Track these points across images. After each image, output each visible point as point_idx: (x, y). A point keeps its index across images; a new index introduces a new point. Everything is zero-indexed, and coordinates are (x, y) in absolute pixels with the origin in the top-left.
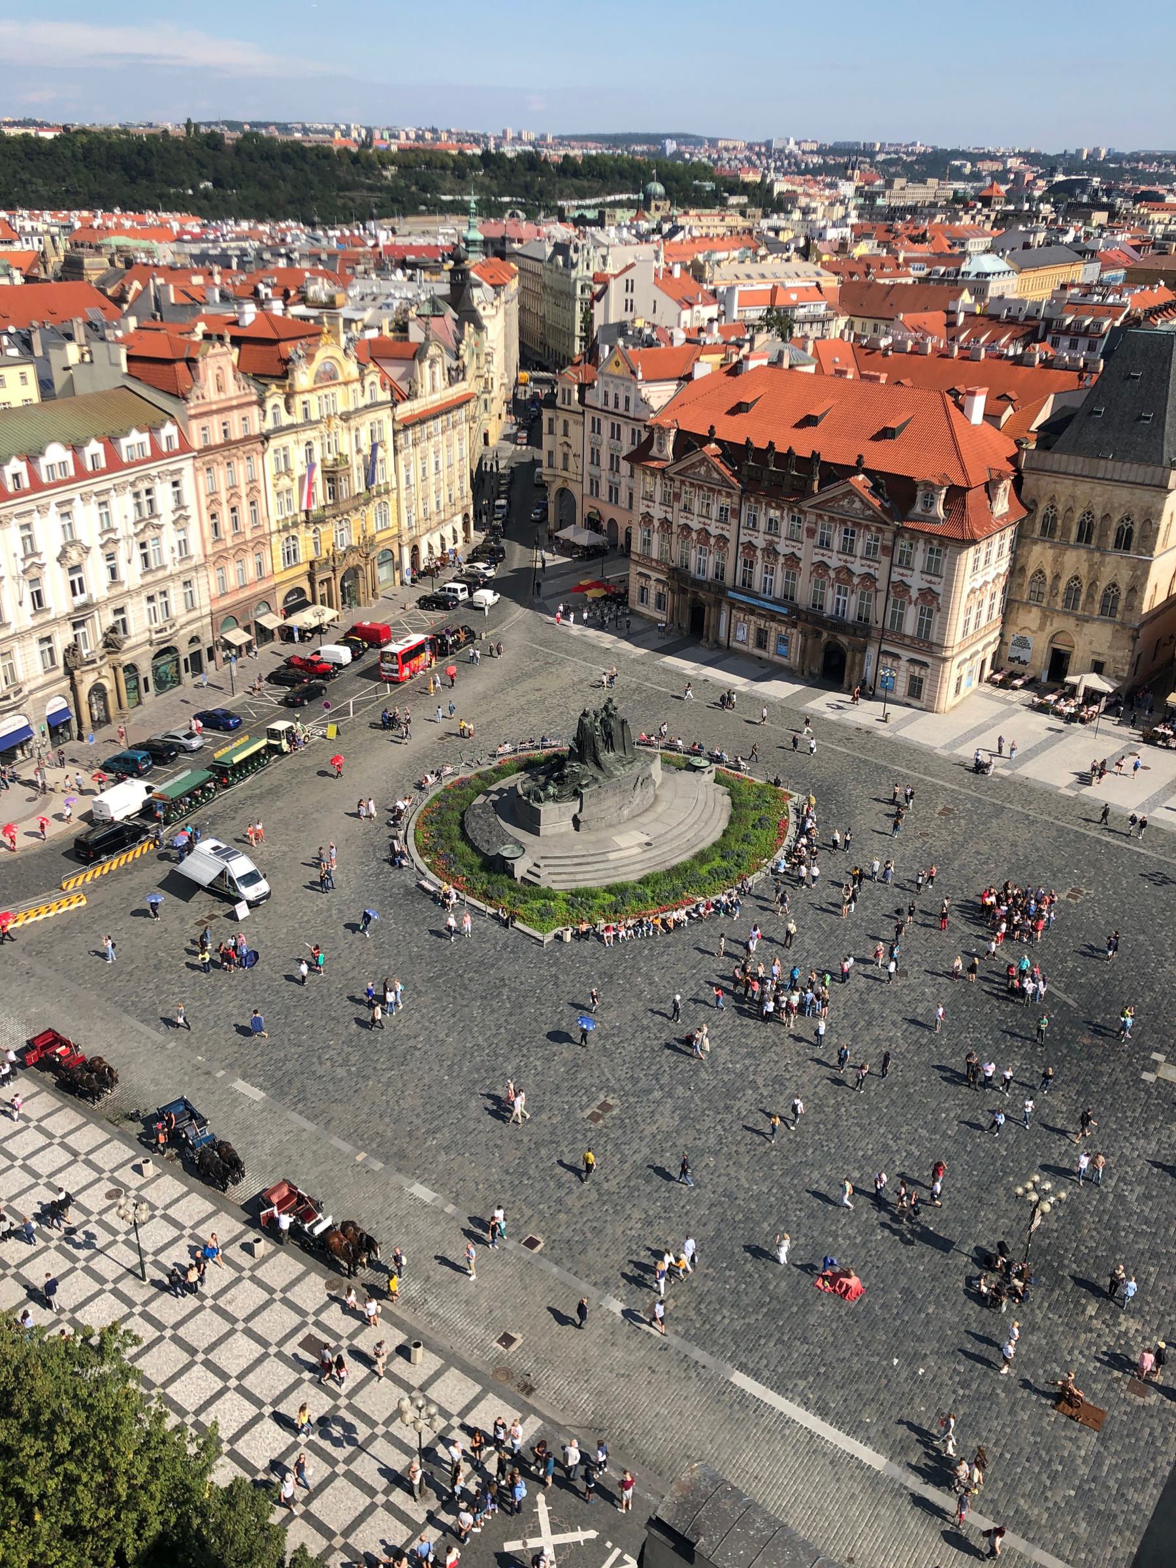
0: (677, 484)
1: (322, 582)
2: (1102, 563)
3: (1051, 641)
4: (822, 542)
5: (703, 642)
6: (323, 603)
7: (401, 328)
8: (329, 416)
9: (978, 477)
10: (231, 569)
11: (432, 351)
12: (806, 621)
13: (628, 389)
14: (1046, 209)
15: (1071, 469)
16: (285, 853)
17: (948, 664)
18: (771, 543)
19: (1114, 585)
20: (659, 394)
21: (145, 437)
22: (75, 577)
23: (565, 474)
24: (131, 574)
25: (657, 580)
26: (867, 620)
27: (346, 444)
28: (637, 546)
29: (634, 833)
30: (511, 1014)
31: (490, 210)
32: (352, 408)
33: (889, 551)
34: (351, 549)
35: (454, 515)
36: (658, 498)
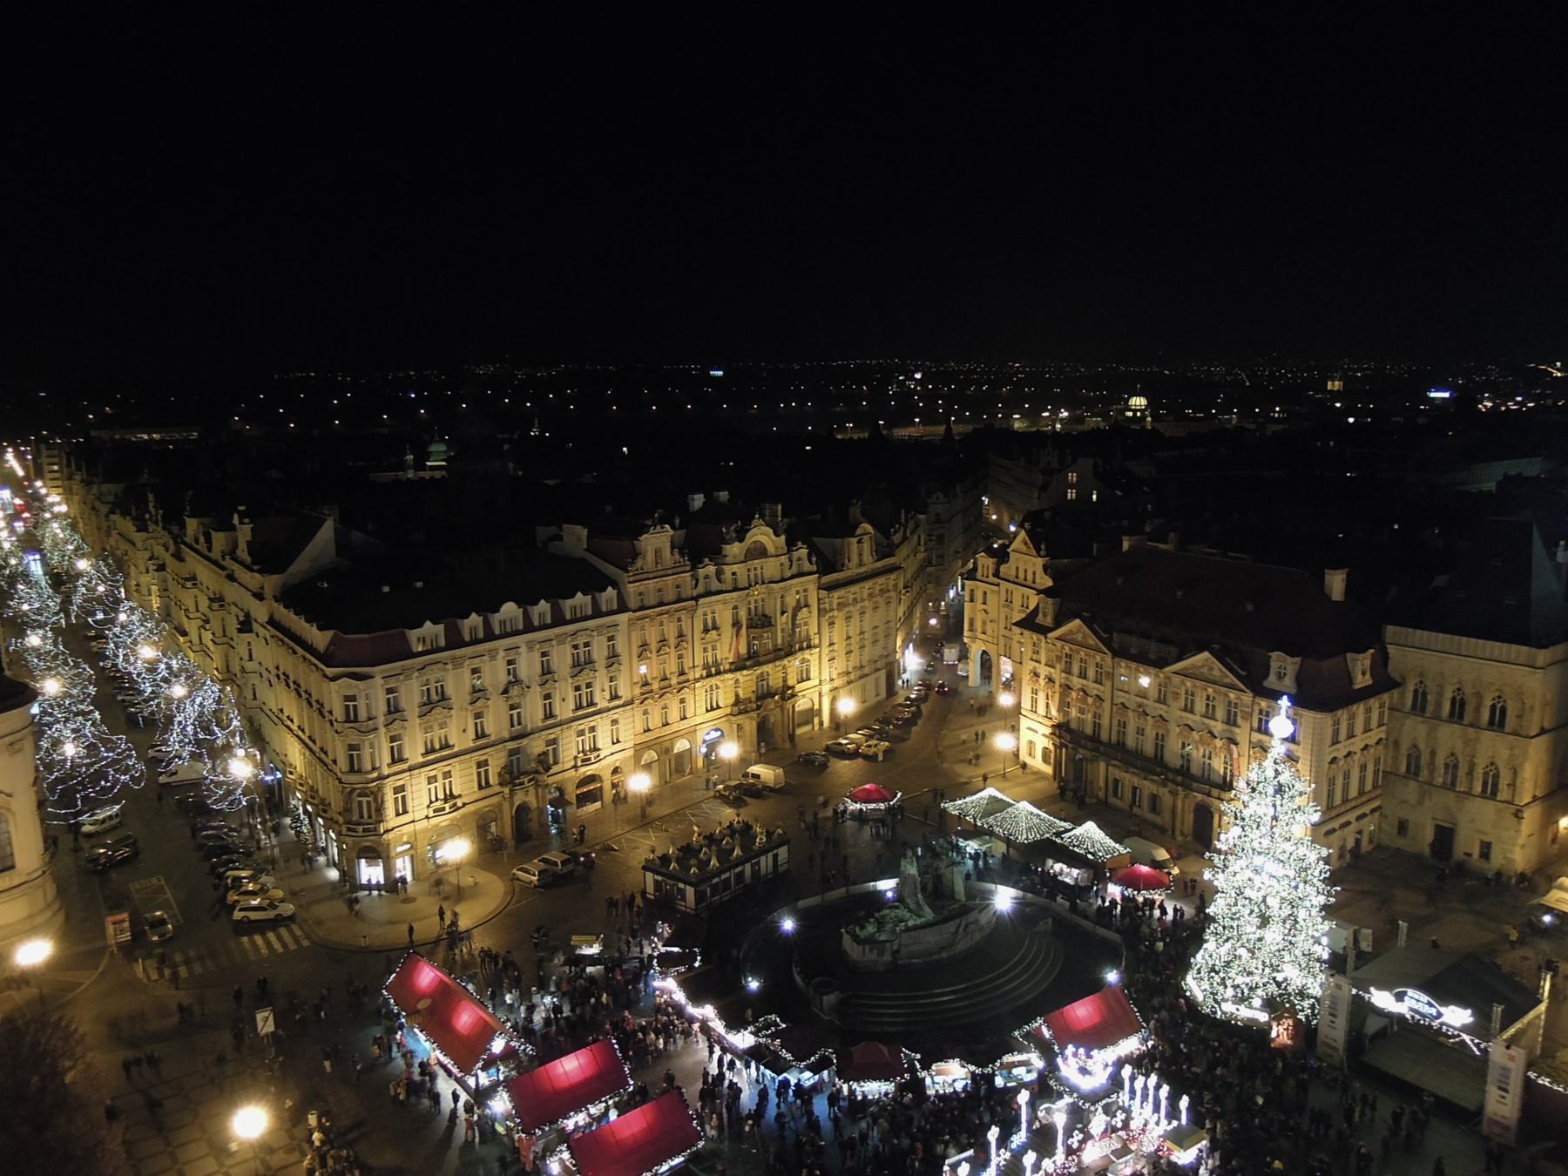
22: (514, 712)
35: (877, 670)
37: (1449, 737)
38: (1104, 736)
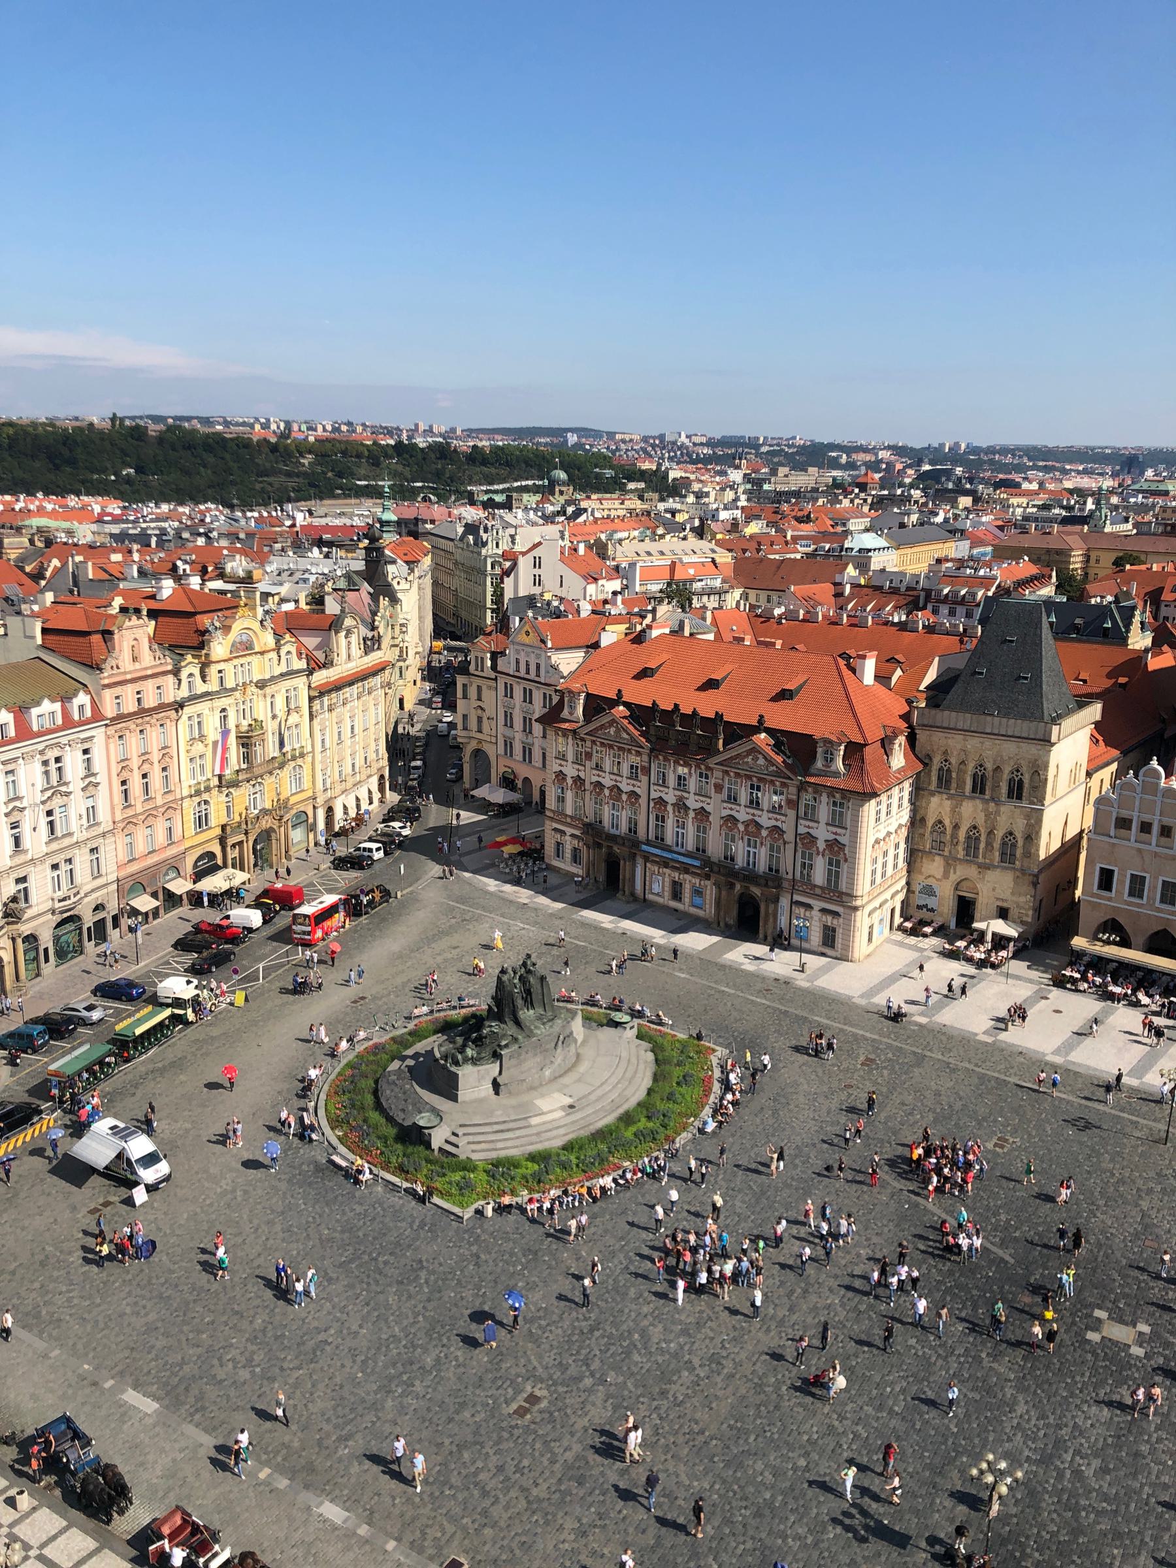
0: (588, 744)
1: (234, 846)
2: (998, 813)
3: (956, 889)
4: (729, 797)
5: (619, 895)
6: (234, 866)
7: (317, 601)
8: (244, 684)
9: (874, 734)
10: (141, 834)
11: (348, 622)
12: (719, 872)
13: (538, 656)
14: (916, 494)
15: (960, 725)
16: (187, 1131)
17: (859, 913)
18: (681, 798)
19: (1011, 834)
20: (568, 662)
21: (57, 706)
23: (479, 736)
24: (36, 841)
25: (572, 835)
26: (777, 871)
27: (261, 710)
28: (551, 803)
29: (556, 1095)
30: (429, 1300)
31: (403, 493)
32: (267, 677)
33: (793, 804)
34: (265, 812)
35: (370, 776)
36: (570, 757)
37: (972, 811)
38: (641, 834)
